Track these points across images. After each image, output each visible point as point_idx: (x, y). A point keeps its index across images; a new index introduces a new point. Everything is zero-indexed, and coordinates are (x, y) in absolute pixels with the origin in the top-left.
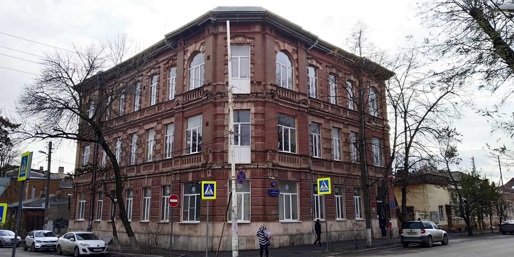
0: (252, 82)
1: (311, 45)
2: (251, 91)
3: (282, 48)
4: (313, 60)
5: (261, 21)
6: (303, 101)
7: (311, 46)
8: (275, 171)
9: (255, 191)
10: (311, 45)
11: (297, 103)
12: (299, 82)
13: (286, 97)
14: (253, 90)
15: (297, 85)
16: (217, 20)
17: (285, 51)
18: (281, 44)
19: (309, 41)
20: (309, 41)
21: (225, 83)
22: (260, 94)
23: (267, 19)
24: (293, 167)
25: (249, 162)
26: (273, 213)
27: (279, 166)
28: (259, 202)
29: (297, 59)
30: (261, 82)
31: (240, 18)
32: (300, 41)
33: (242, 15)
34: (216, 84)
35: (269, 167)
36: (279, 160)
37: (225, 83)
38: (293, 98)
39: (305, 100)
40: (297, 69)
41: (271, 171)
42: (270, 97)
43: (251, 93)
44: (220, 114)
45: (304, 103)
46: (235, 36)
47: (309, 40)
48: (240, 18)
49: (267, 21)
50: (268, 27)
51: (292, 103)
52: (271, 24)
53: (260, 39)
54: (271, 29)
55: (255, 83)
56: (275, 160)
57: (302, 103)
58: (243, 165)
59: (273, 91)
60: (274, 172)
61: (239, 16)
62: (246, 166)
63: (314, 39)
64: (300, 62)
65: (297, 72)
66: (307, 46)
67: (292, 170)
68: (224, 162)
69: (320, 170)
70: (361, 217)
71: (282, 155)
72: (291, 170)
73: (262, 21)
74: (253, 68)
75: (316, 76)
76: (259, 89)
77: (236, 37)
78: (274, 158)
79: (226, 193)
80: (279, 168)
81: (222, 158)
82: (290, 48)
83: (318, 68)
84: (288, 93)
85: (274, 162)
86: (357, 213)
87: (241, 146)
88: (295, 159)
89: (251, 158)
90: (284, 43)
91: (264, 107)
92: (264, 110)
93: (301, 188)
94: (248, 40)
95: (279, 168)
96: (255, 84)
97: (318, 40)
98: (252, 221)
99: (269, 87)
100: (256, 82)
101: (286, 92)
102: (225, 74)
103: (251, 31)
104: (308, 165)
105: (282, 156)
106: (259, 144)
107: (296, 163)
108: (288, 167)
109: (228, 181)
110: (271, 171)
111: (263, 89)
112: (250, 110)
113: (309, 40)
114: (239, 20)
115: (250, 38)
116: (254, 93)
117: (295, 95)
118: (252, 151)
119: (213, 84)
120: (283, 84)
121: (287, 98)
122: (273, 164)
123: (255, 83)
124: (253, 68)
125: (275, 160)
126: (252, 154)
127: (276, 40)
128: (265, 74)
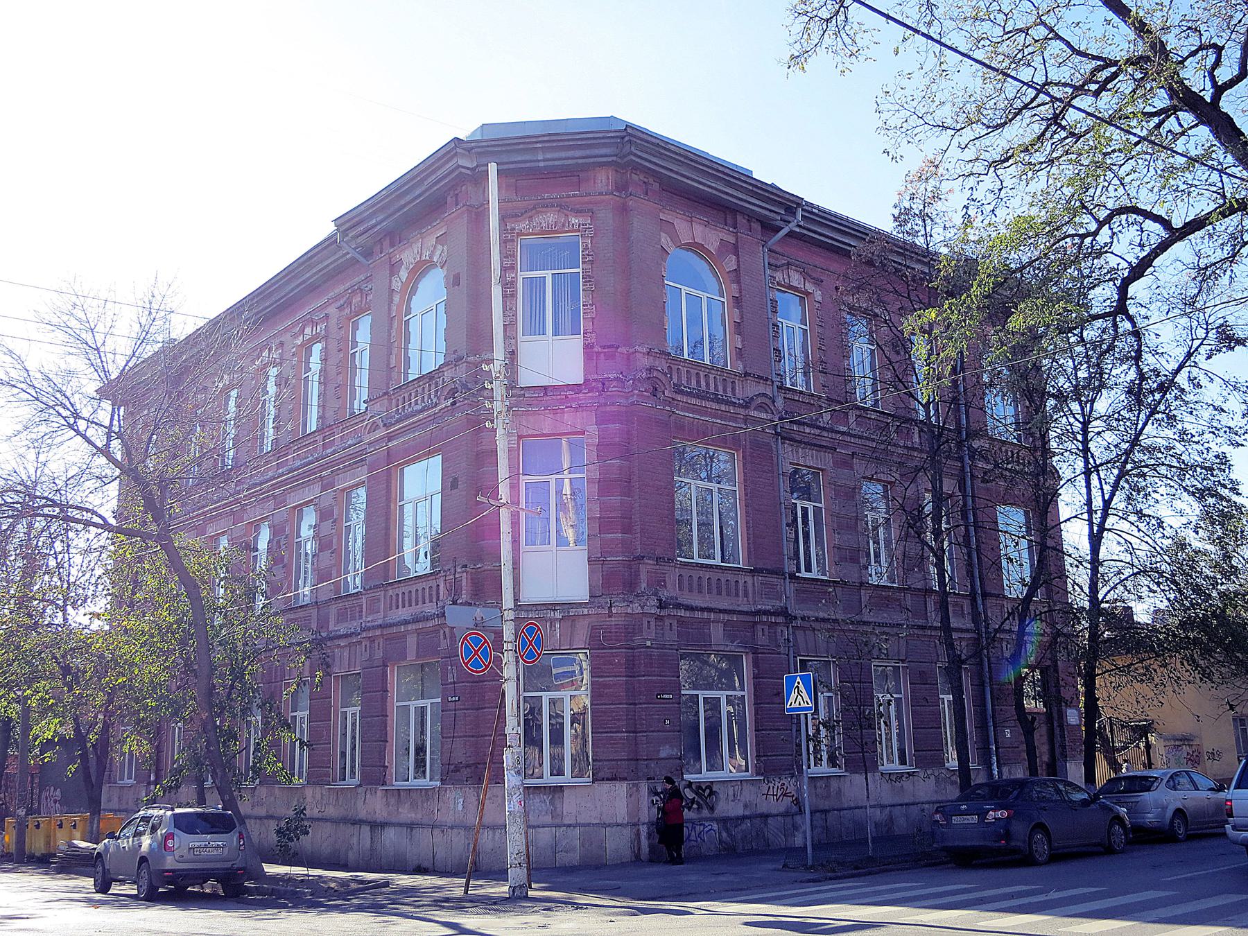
0: (587, 347)
4: (792, 273)
6: (760, 400)
8: (667, 622)
9: (605, 686)
11: (740, 406)
15: (739, 353)
17: (696, 248)
18: (681, 225)
19: (772, 215)
20: (772, 215)
22: (615, 383)
26: (663, 754)
27: (678, 606)
28: (619, 720)
35: (647, 609)
36: (681, 589)
39: (765, 395)
41: (653, 624)
45: (760, 407)
48: (549, 156)
57: (753, 405)
63: (791, 204)
64: (745, 279)
66: (769, 228)
67: (727, 617)
73: (614, 158)
74: (591, 305)
75: (803, 322)
77: (538, 213)
80: (682, 613)
83: (807, 294)
85: (664, 594)
94: (574, 221)
96: (598, 353)
100: (604, 347)
108: (710, 610)
110: (653, 624)
114: (544, 160)
115: (578, 212)
124: (591, 305)
126: (591, 572)
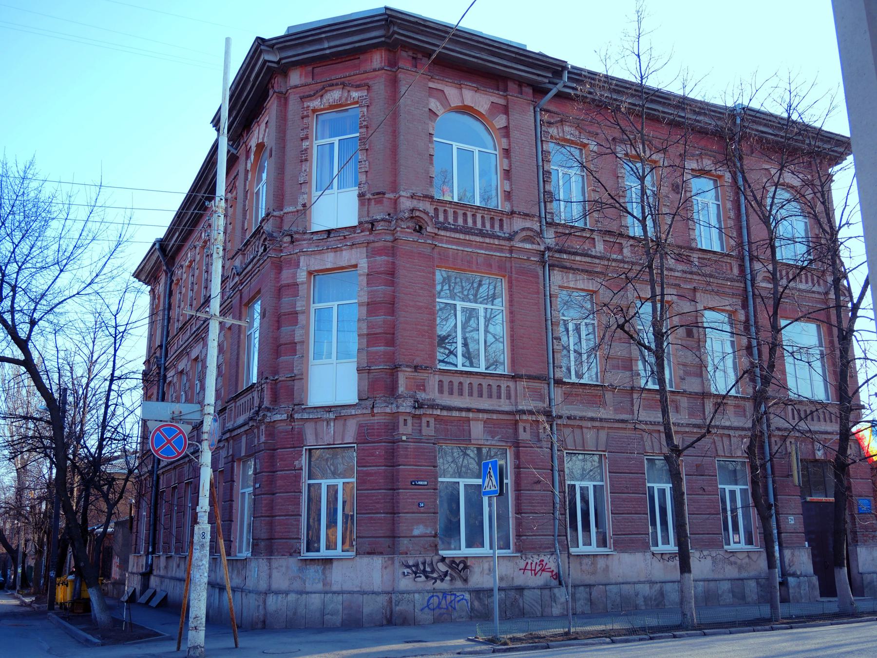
0: (361, 196)
1: (550, 86)
2: (359, 218)
3: (455, 102)
4: (567, 129)
5: (382, 42)
6: (524, 233)
7: (551, 89)
8: (424, 420)
9: (369, 474)
10: (550, 86)
11: (505, 239)
12: (511, 185)
13: (468, 228)
14: (363, 217)
15: (508, 196)
16: (281, 59)
17: (466, 110)
18: (451, 92)
19: (540, 79)
20: (540, 79)
21: (300, 207)
22: (382, 223)
23: (395, 33)
24: (490, 408)
25: (352, 398)
26: (416, 532)
27: (433, 406)
28: (378, 503)
29: (507, 128)
30: (384, 194)
31: (332, 44)
32: (529, 85)
33: (335, 33)
34: (282, 213)
35: (401, 409)
36: (441, 391)
37: (300, 207)
38: (492, 226)
39: (528, 229)
40: (507, 152)
41: (410, 422)
42: (408, 228)
43: (360, 223)
44: (288, 285)
45: (526, 239)
46: (324, 88)
47: (539, 75)
48: (332, 44)
49: (396, 36)
50: (404, 54)
51: (487, 240)
52: (406, 42)
53: (383, 87)
54: (413, 58)
55: (368, 196)
56: (424, 390)
57: (517, 238)
58: (339, 409)
59: (417, 214)
60: (421, 423)
61: (328, 39)
62: (344, 412)
63: (557, 68)
64: (514, 134)
65: (506, 161)
66: (539, 91)
67: (486, 416)
68: (295, 405)
69: (590, 414)
70: (749, 541)
71: (462, 379)
72: (481, 415)
73: (383, 39)
74: (365, 161)
76: (378, 213)
77: (326, 92)
78: (424, 386)
79: (300, 482)
80: (438, 412)
81: (291, 393)
82: (482, 101)
83: (585, 145)
84: (474, 216)
85: (421, 396)
86: (736, 529)
87: (338, 361)
88: (499, 386)
89: (358, 390)
90: (461, 88)
91: (393, 257)
92: (393, 263)
93: (519, 464)
94: (355, 94)
95: (438, 412)
96: (369, 199)
97: (569, 72)
98: (358, 554)
99: (406, 204)
100: (373, 195)
101: (469, 214)
102: (301, 184)
103: (362, 70)
104: (544, 402)
105: (470, 383)
106: (376, 353)
107: (499, 397)
108: (468, 410)
109: (304, 452)
110: (410, 422)
111: (391, 211)
112: (355, 266)
113: (539, 75)
114: (329, 48)
115: (358, 87)
116: (367, 222)
117: (501, 220)
118: (359, 370)
119: (275, 214)
120: (483, 199)
121: (472, 228)
122: (416, 401)
123: (368, 196)
124: (365, 161)
125: (424, 390)
126: (360, 380)
127: (431, 85)
128: (395, 172)
